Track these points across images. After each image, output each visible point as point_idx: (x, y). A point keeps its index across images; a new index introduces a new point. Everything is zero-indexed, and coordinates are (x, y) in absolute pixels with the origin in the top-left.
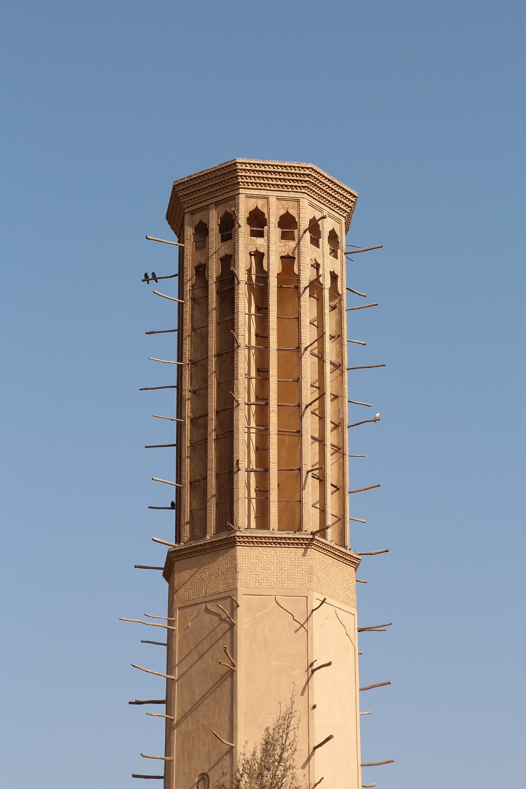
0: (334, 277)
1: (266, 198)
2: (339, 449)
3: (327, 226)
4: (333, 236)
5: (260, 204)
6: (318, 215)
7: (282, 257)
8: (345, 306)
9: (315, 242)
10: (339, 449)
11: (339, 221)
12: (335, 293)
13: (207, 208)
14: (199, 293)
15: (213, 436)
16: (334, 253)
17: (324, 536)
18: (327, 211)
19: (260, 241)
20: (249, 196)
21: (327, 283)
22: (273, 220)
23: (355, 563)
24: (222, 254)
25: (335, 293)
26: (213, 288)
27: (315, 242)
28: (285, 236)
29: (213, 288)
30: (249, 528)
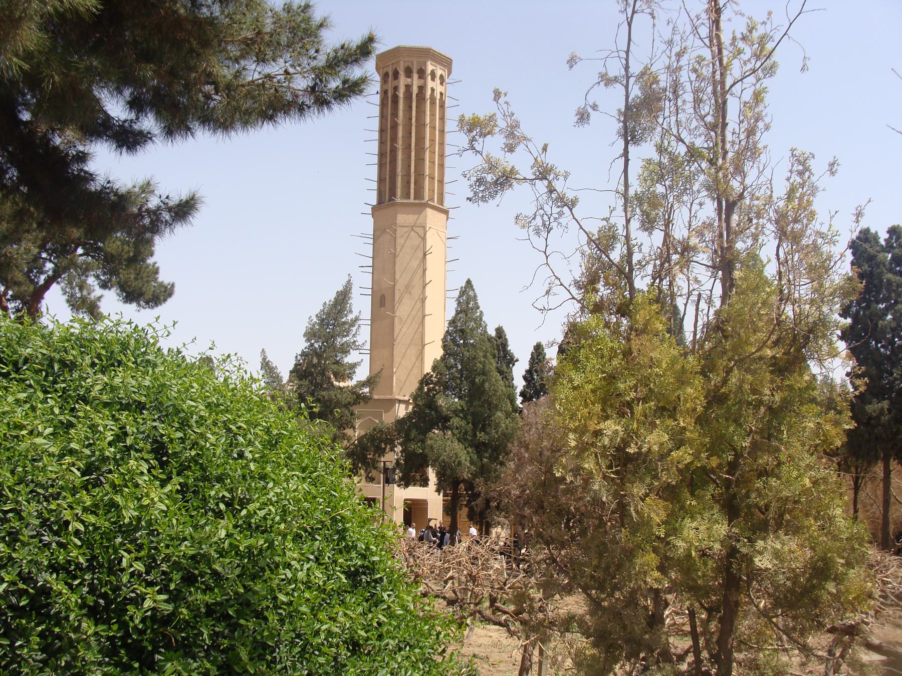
3: (439, 72)
4: (441, 77)
6: (434, 68)
9: (433, 79)
11: (444, 71)
13: (389, 66)
14: (385, 102)
16: (442, 84)
18: (439, 66)
19: (409, 80)
20: (405, 61)
21: (438, 97)
22: (415, 70)
23: (446, 212)
24: (393, 86)
27: (433, 79)
28: (420, 78)
29: (390, 99)
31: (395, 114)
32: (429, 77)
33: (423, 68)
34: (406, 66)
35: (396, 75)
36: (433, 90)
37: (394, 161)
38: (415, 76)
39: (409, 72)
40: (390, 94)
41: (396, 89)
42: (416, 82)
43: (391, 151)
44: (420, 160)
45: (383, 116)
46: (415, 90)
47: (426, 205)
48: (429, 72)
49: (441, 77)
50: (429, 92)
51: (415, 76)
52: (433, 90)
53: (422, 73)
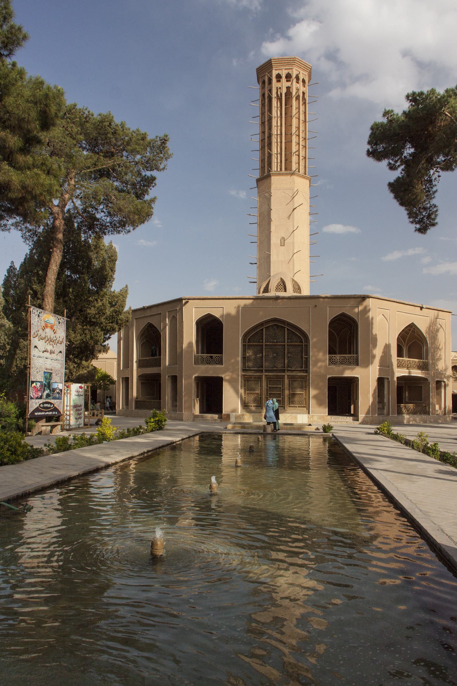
0: (304, 93)
1: (282, 69)
2: (305, 147)
3: (301, 78)
5: (280, 72)
7: (287, 87)
8: (307, 102)
9: (298, 82)
10: (305, 147)
12: (304, 99)
13: (265, 75)
15: (266, 145)
17: (299, 172)
18: (301, 72)
25: (304, 99)
26: (266, 100)
27: (298, 82)
28: (287, 81)
29: (266, 100)
30: (277, 171)
31: (270, 110)
32: (295, 80)
33: (291, 73)
34: (277, 72)
35: (270, 81)
36: (298, 90)
37: (270, 144)
38: (284, 79)
39: (279, 77)
40: (266, 96)
41: (270, 91)
42: (284, 84)
43: (268, 137)
44: (289, 142)
45: (263, 114)
46: (284, 91)
47: (292, 174)
48: (294, 76)
49: (304, 81)
50: (294, 93)
51: (284, 79)
52: (298, 90)
53: (288, 77)
